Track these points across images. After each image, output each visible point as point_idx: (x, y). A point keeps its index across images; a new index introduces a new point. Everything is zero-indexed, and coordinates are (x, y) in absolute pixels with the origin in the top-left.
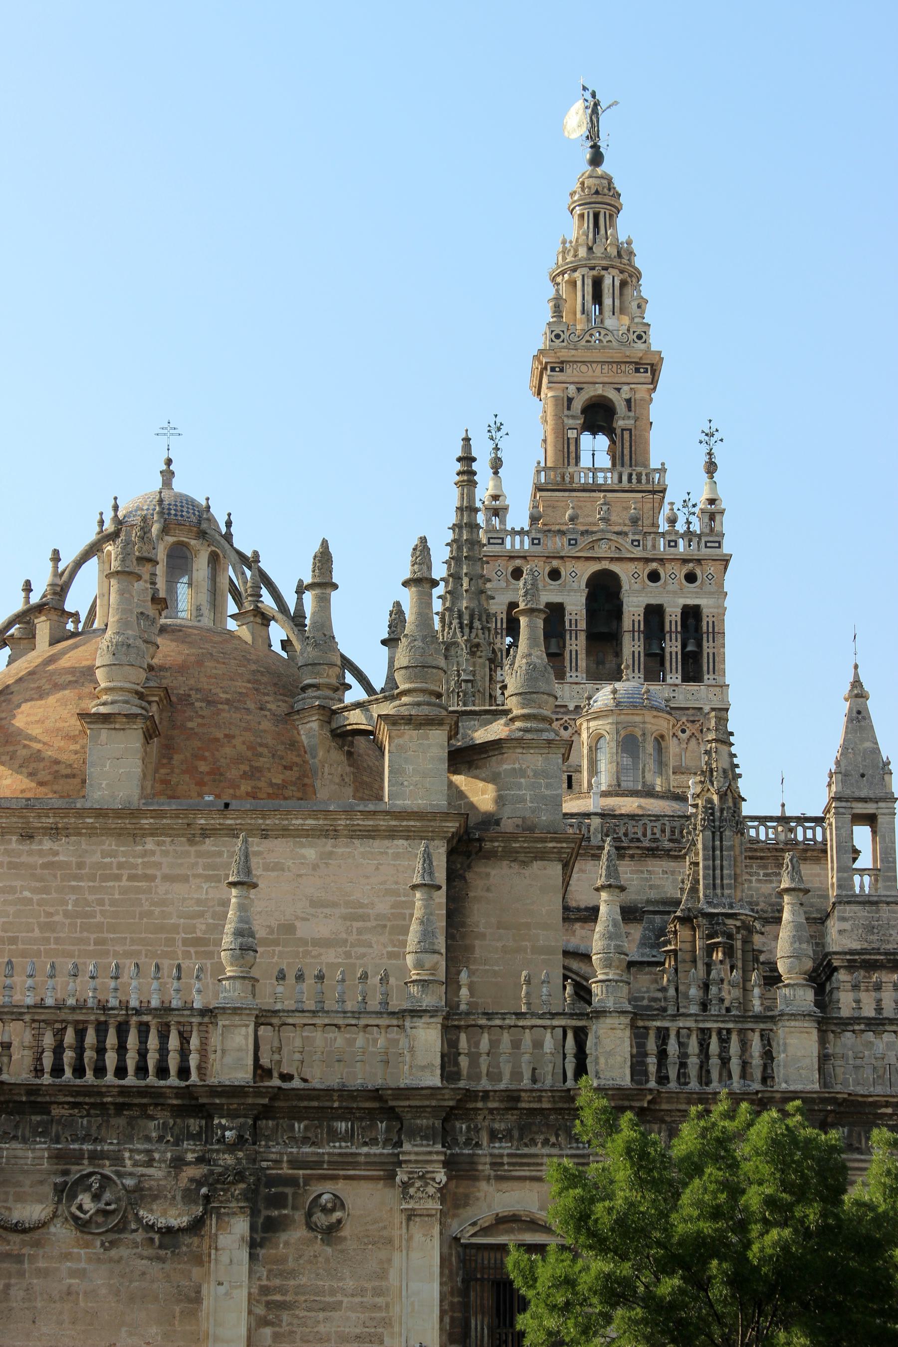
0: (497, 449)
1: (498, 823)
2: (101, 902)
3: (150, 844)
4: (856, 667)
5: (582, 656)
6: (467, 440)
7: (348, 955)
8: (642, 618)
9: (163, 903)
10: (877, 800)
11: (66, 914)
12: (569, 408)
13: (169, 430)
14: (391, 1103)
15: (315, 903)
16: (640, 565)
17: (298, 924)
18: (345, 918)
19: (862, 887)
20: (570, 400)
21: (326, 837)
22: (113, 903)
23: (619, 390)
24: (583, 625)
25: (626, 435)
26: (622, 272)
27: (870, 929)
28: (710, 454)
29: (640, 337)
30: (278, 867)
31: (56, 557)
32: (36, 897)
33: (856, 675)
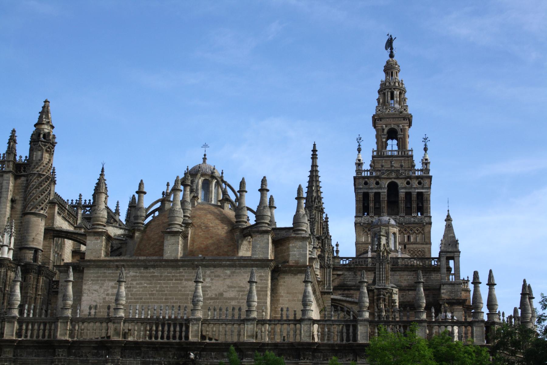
0: (359, 145)
2: (167, 287)
4: (448, 211)
5: (386, 208)
6: (314, 145)
7: (239, 302)
9: (185, 287)
10: (454, 252)
11: (157, 291)
12: (383, 132)
14: (240, 347)
15: (229, 287)
17: (224, 293)
18: (238, 291)
19: (452, 279)
20: (383, 130)
21: (233, 267)
23: (398, 126)
24: (386, 199)
25: (401, 140)
26: (400, 89)
27: (451, 292)
28: (425, 145)
30: (219, 276)
32: (148, 286)
33: (448, 213)
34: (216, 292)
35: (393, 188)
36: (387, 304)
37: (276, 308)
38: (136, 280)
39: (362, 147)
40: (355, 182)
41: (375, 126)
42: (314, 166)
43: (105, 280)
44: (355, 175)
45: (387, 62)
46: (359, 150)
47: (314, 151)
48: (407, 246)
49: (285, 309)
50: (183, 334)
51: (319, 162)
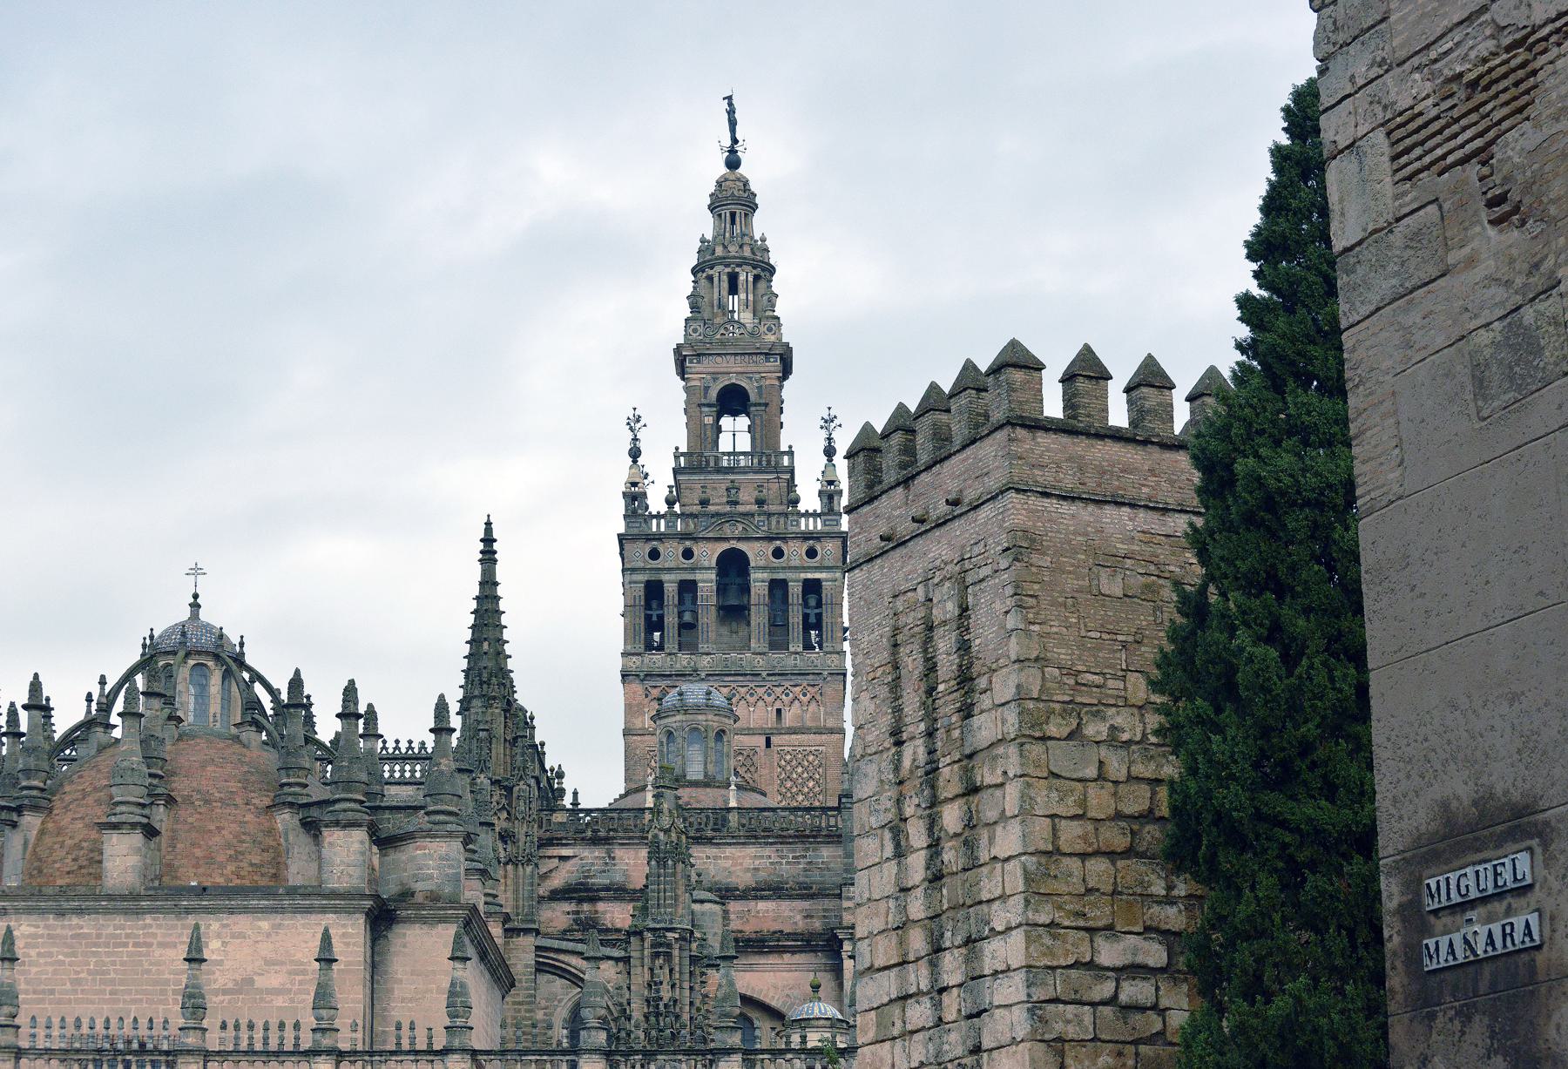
0: (635, 439)
1: (413, 894)
2: (114, 963)
3: (148, 919)
5: (713, 627)
6: (488, 524)
7: (292, 1000)
9: (158, 963)
11: (89, 972)
13: (196, 571)
15: (269, 962)
16: (764, 544)
18: (290, 973)
20: (707, 389)
22: (123, 964)
24: (714, 601)
28: (829, 439)
29: (770, 329)
30: (242, 936)
31: (103, 681)
34: (239, 978)
35: (733, 566)
37: (385, 1010)
38: (35, 946)
39: (642, 445)
40: (622, 549)
41: (682, 371)
42: (488, 583)
44: (622, 531)
45: (719, 184)
46: (635, 454)
47: (488, 540)
51: (501, 573)
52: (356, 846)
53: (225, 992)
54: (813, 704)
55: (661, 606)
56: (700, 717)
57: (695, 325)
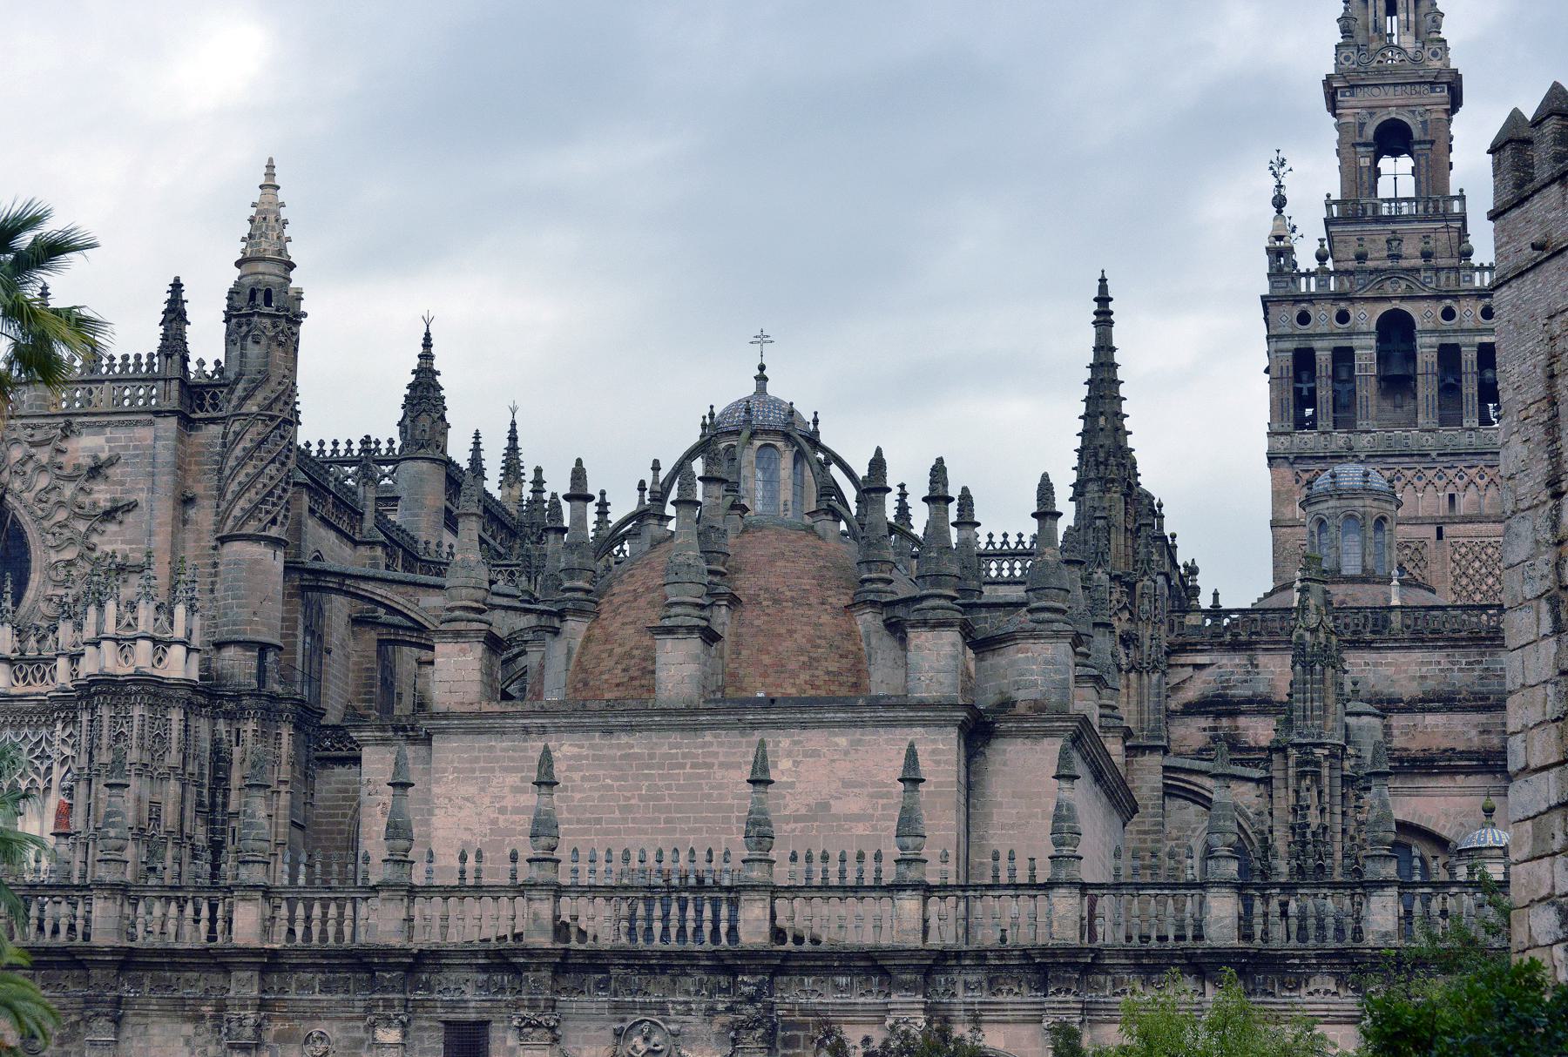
0: (1280, 186)
1: (1014, 704)
2: (669, 787)
3: (708, 736)
5: (1373, 401)
6: (1103, 280)
7: (874, 828)
8: (1435, 359)
9: (720, 786)
11: (641, 798)
15: (847, 784)
20: (1362, 125)
22: (679, 787)
29: (1435, 54)
30: (815, 754)
31: (656, 467)
35: (1396, 330)
36: (1327, 790)
38: (579, 769)
39: (1285, 192)
41: (1333, 106)
42: (1104, 349)
43: (493, 770)
44: (1267, 292)
46: (1279, 203)
47: (1103, 299)
48: (1447, 530)
49: (1004, 856)
50: (724, 927)
52: (948, 650)
53: (797, 819)
54: (1492, 486)
55: (1313, 378)
56: (1357, 503)
57: (1346, 52)
